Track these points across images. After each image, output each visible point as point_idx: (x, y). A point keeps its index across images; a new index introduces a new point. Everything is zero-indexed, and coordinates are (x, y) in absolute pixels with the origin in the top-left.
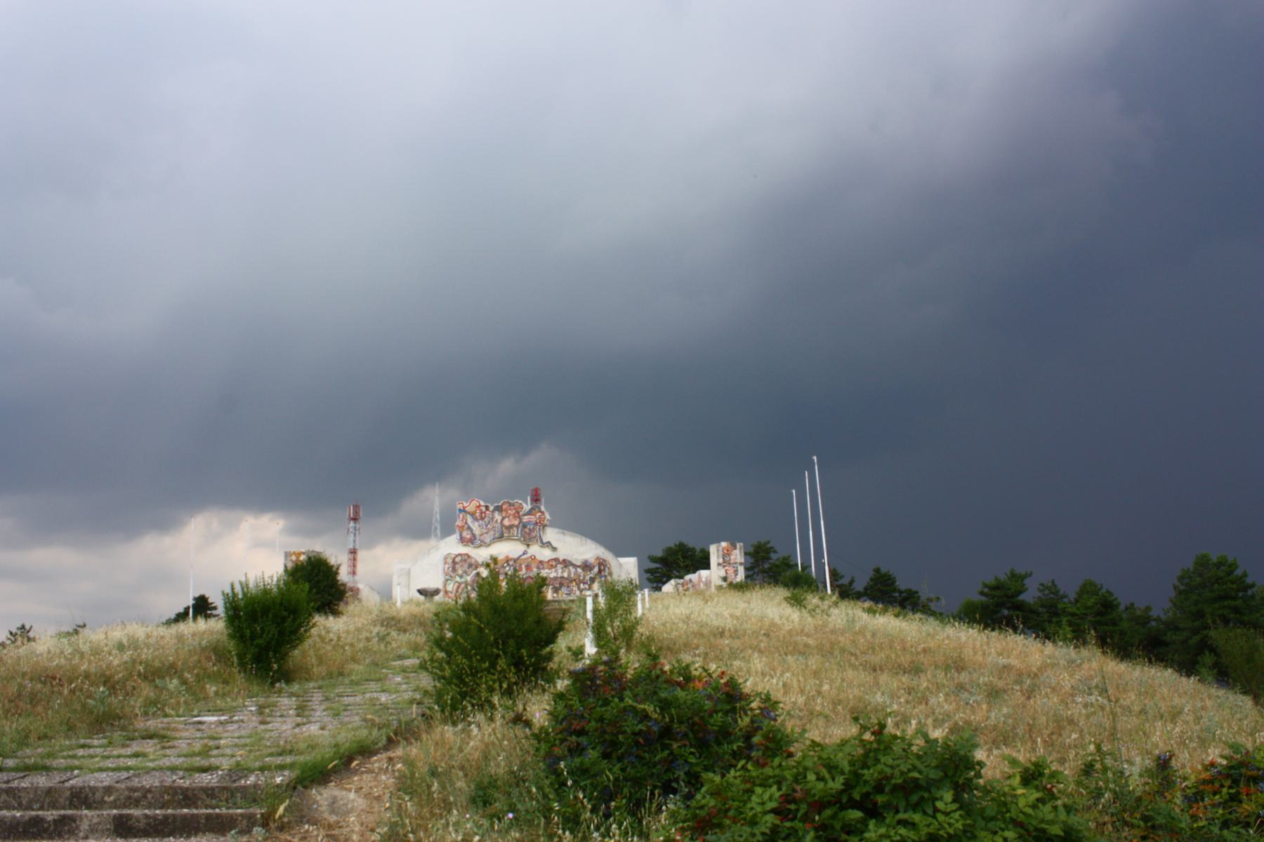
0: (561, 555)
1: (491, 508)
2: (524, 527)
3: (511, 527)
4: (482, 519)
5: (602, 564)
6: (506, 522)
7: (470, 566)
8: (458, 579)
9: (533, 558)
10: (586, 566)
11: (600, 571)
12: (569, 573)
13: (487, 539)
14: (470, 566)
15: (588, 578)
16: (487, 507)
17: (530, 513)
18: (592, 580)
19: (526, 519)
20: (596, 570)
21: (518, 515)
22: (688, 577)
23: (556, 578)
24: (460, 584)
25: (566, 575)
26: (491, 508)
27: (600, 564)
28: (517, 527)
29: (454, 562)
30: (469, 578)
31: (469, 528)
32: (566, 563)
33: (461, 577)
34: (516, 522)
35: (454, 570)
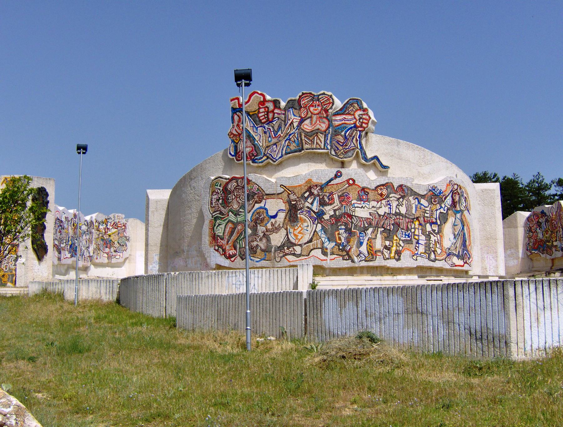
0: (396, 176)
1: (283, 104)
2: (336, 133)
3: (315, 133)
4: (269, 122)
5: (457, 192)
6: (307, 126)
7: (251, 196)
8: (232, 217)
9: (351, 182)
10: (434, 195)
11: (454, 204)
12: (409, 208)
13: (277, 152)
14: (251, 196)
15: (437, 214)
16: (276, 103)
17: (342, 111)
18: (444, 218)
19: (338, 120)
20: (449, 201)
21: (325, 113)
22: (538, 209)
23: (387, 216)
24: (235, 224)
25: (403, 210)
26: (283, 104)
27: (453, 193)
28: (325, 133)
29: (225, 190)
30: (249, 216)
31: (249, 136)
32: (404, 191)
33: (236, 214)
34: (323, 127)
35: (226, 202)
